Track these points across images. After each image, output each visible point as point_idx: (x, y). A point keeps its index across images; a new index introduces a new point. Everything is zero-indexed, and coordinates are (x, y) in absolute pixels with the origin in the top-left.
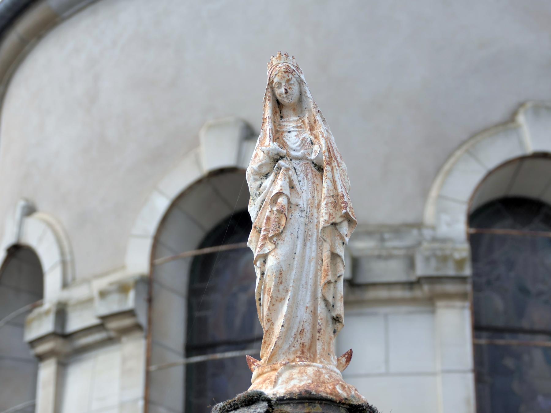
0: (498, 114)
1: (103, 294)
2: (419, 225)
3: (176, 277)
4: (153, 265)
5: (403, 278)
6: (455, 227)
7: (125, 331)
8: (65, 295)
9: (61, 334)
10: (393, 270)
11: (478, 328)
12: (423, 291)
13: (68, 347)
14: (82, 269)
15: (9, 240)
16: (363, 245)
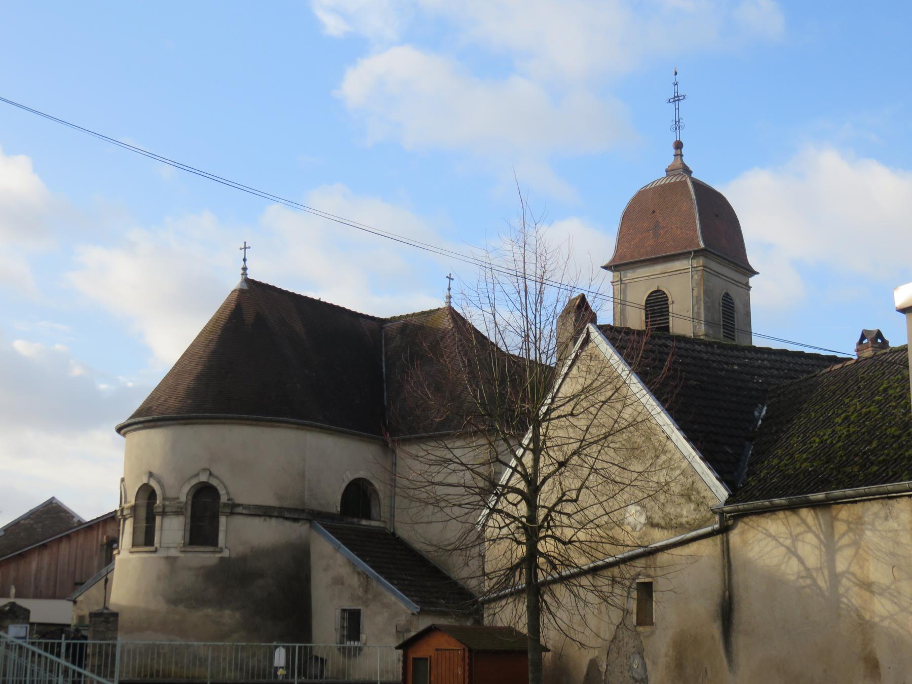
0: (196, 473)
12: (178, 513)
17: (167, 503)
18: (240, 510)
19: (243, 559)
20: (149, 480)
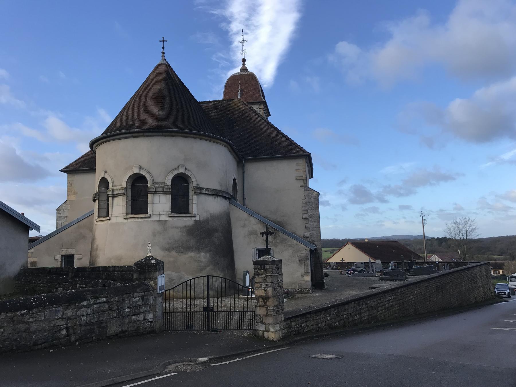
0: (176, 167)
2: (165, 183)
3: (129, 186)
6: (169, 183)
10: (161, 190)
12: (165, 193)
13: (114, 196)
16: (156, 186)
17: (156, 186)
18: (204, 191)
19: (207, 221)
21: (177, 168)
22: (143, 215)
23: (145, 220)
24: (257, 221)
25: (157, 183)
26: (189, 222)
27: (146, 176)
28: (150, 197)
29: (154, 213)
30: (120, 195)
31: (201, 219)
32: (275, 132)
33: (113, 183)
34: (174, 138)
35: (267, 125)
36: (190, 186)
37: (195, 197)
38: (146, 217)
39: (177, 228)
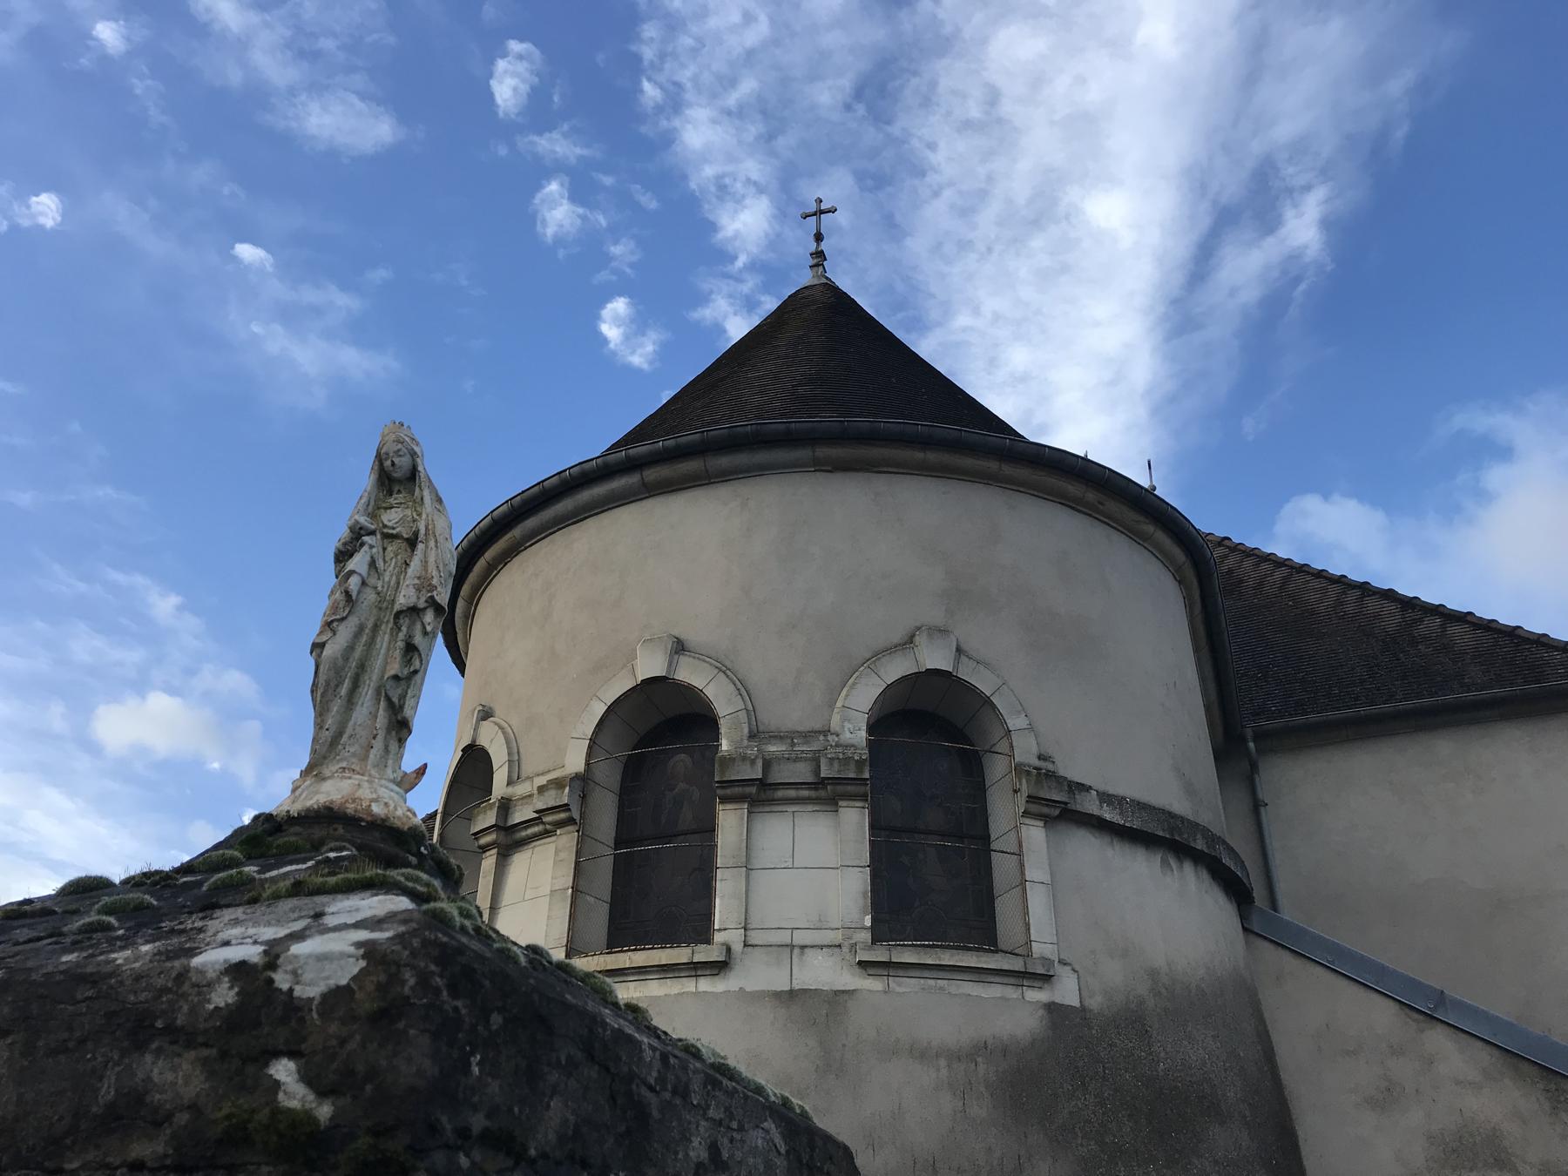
0: (896, 637)
1: (541, 789)
2: (826, 732)
3: (609, 775)
4: (588, 764)
5: (810, 780)
6: (855, 733)
7: (561, 824)
8: (510, 790)
9: (503, 828)
10: (802, 772)
11: (873, 827)
12: (826, 793)
14: (527, 769)
15: (466, 742)
16: (773, 748)
17: (773, 748)
18: (1090, 805)
19: (1131, 1020)
20: (671, 664)
21: (910, 641)
22: (680, 955)
23: (689, 985)
24: (1485, 1055)
25: (778, 737)
26: (1013, 1015)
27: (710, 692)
28: (729, 822)
29: (756, 937)
30: (545, 825)
31: (1095, 1003)
32: (1392, 607)
33: (514, 762)
34: (880, 483)
35: (1334, 590)
36: (997, 769)
37: (1035, 834)
38: (695, 969)
39: (923, 1054)
